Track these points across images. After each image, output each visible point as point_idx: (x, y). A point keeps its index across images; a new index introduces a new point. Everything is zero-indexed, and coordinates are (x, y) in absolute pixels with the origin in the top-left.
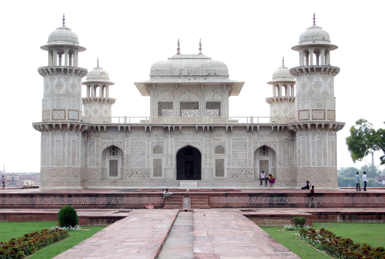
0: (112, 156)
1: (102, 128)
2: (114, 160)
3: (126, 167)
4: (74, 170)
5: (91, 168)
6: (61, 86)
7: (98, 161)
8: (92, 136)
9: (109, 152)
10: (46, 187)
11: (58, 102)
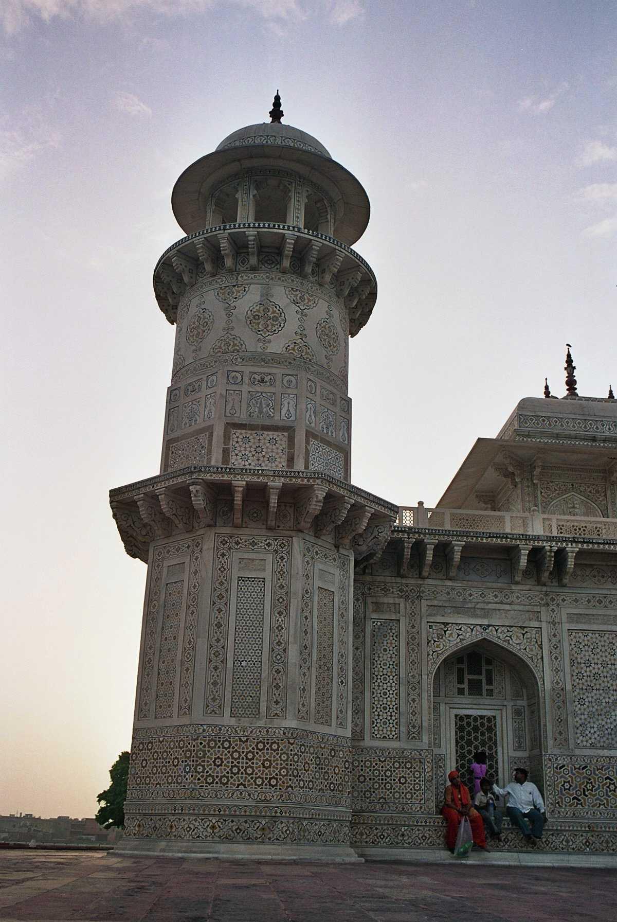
0: (466, 699)
1: (443, 550)
2: (475, 719)
3: (557, 751)
4: (326, 752)
5: (382, 750)
6: (275, 319)
7: (414, 713)
8: (385, 590)
9: (454, 677)
10: (163, 844)
11: (258, 388)
